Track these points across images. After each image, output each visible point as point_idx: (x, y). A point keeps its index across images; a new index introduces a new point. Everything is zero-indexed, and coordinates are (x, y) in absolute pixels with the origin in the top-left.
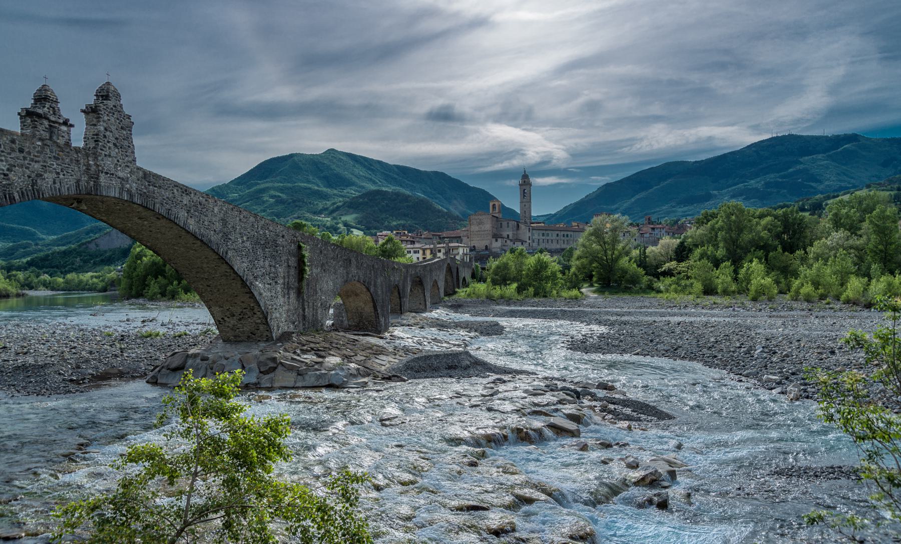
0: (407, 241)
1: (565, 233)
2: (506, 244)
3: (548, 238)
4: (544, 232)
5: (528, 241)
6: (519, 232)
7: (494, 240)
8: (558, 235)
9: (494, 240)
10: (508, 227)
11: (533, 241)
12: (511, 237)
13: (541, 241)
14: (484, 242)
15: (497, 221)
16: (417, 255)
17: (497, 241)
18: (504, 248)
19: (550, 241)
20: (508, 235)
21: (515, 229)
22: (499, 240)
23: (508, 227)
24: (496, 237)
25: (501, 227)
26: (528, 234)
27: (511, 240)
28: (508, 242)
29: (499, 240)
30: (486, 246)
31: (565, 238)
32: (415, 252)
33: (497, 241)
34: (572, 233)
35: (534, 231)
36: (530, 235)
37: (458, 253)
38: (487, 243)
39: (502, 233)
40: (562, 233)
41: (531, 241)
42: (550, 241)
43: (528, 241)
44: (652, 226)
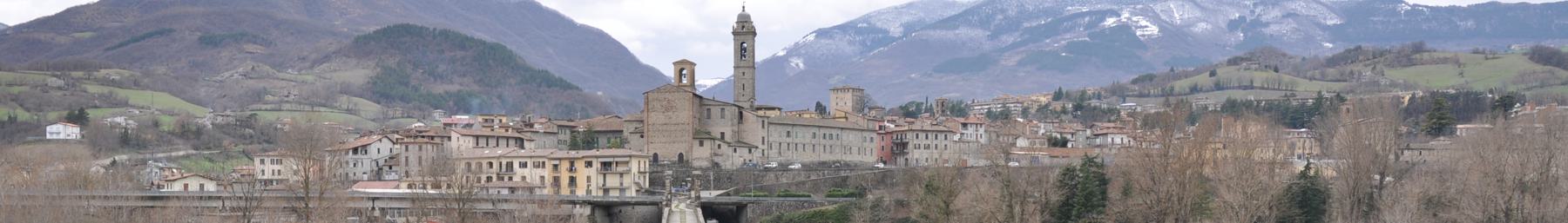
0: (508, 138)
1: (828, 132)
2: (719, 152)
3: (797, 141)
4: (790, 129)
5: (761, 146)
6: (742, 127)
8: (814, 135)
9: (697, 142)
10: (723, 117)
12: (728, 138)
13: (784, 146)
14: (676, 145)
15: (701, 105)
16: (540, 171)
17: (701, 144)
18: (716, 159)
19: (800, 147)
20: (723, 134)
21: (736, 121)
22: (707, 143)
23: (723, 117)
24: (701, 136)
25: (709, 117)
26: (762, 133)
28: (724, 147)
30: (681, 156)
31: (828, 142)
32: (536, 166)
33: (701, 144)
34: (839, 132)
35: (772, 128)
36: (765, 135)
37: (629, 172)
38: (681, 148)
39: (709, 129)
40: (823, 131)
41: (765, 147)
42: (800, 147)
43: (761, 146)
44: (962, 120)
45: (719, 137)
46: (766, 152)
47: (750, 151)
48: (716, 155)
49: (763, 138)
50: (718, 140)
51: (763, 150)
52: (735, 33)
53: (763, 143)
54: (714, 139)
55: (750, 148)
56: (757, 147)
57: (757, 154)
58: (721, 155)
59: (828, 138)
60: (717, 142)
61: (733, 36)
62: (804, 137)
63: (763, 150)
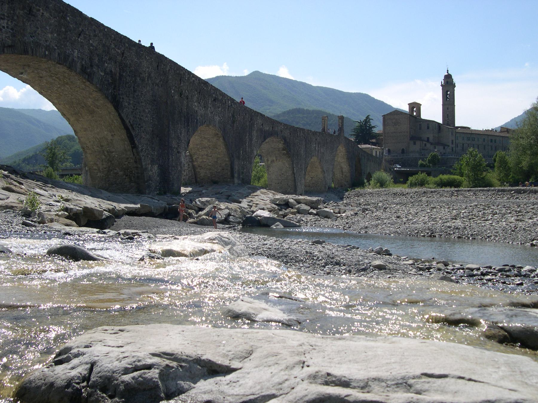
7: (412, 142)
11: (457, 146)
12: (431, 139)
17: (415, 144)
20: (428, 138)
25: (420, 128)
27: (431, 144)
28: (428, 145)
29: (418, 143)
30: (403, 150)
33: (415, 144)
36: (454, 139)
41: (454, 146)
45: (426, 139)
46: (454, 149)
47: (444, 148)
48: (423, 149)
49: (452, 141)
50: (425, 141)
51: (452, 148)
52: (442, 85)
53: (452, 143)
54: (423, 141)
55: (444, 146)
56: (449, 146)
57: (448, 150)
58: (427, 150)
59: (494, 142)
60: (424, 142)
61: (441, 88)
62: (478, 140)
63: (452, 148)
